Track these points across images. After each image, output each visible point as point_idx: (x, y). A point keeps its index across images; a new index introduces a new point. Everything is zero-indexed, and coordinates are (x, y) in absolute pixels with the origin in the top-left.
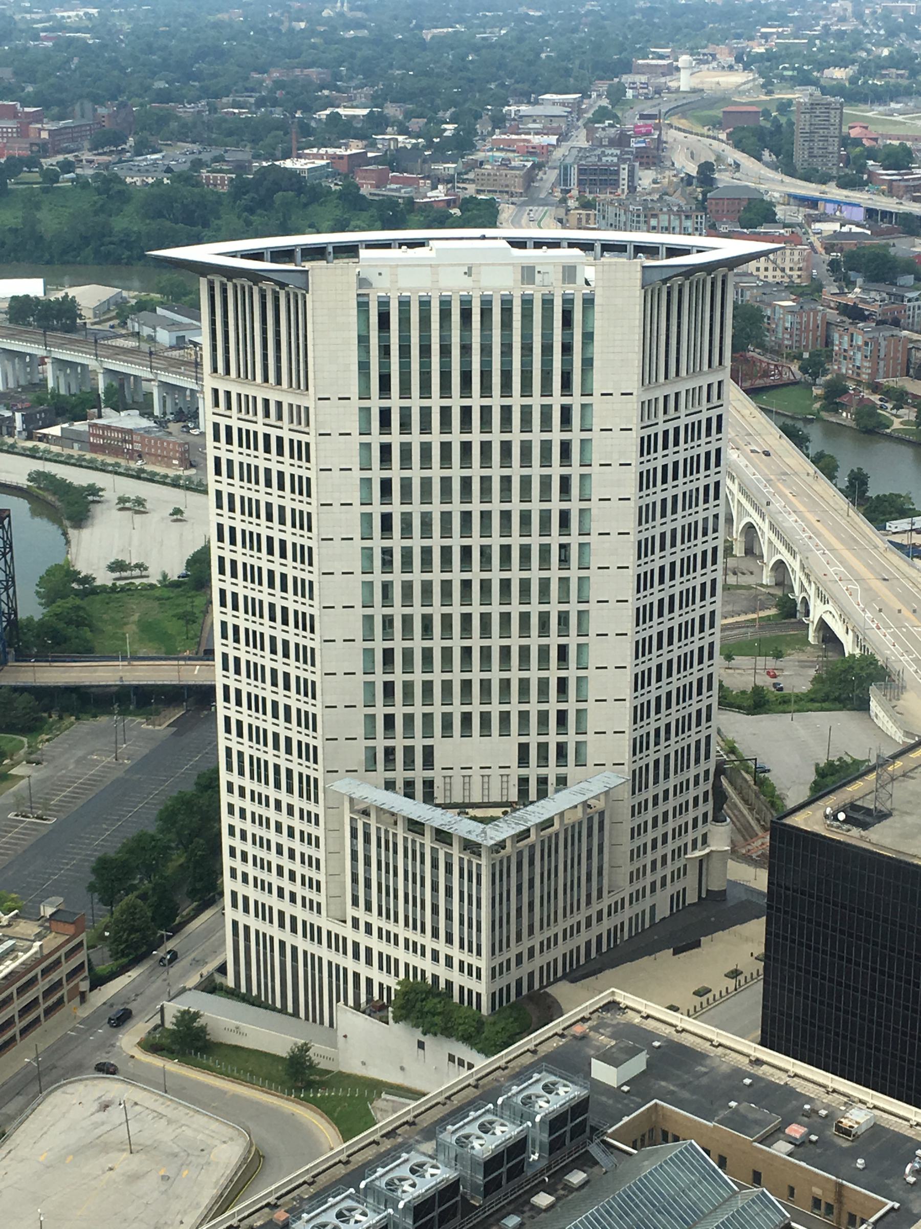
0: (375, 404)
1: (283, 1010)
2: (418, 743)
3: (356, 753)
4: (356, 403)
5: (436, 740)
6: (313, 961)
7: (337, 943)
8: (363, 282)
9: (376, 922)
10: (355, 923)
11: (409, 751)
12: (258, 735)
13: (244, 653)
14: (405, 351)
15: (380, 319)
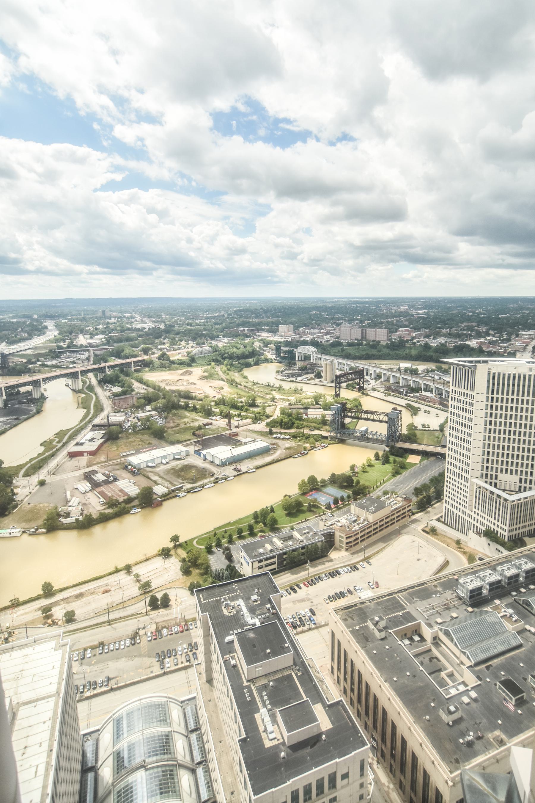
0: (490, 396)
1: (455, 529)
2: (494, 473)
3: (479, 473)
4: (485, 395)
5: (499, 474)
6: (463, 519)
7: (470, 516)
8: (489, 369)
9: (480, 513)
10: (475, 512)
11: (491, 475)
12: (455, 466)
13: (454, 447)
14: (498, 384)
15: (493, 378)
